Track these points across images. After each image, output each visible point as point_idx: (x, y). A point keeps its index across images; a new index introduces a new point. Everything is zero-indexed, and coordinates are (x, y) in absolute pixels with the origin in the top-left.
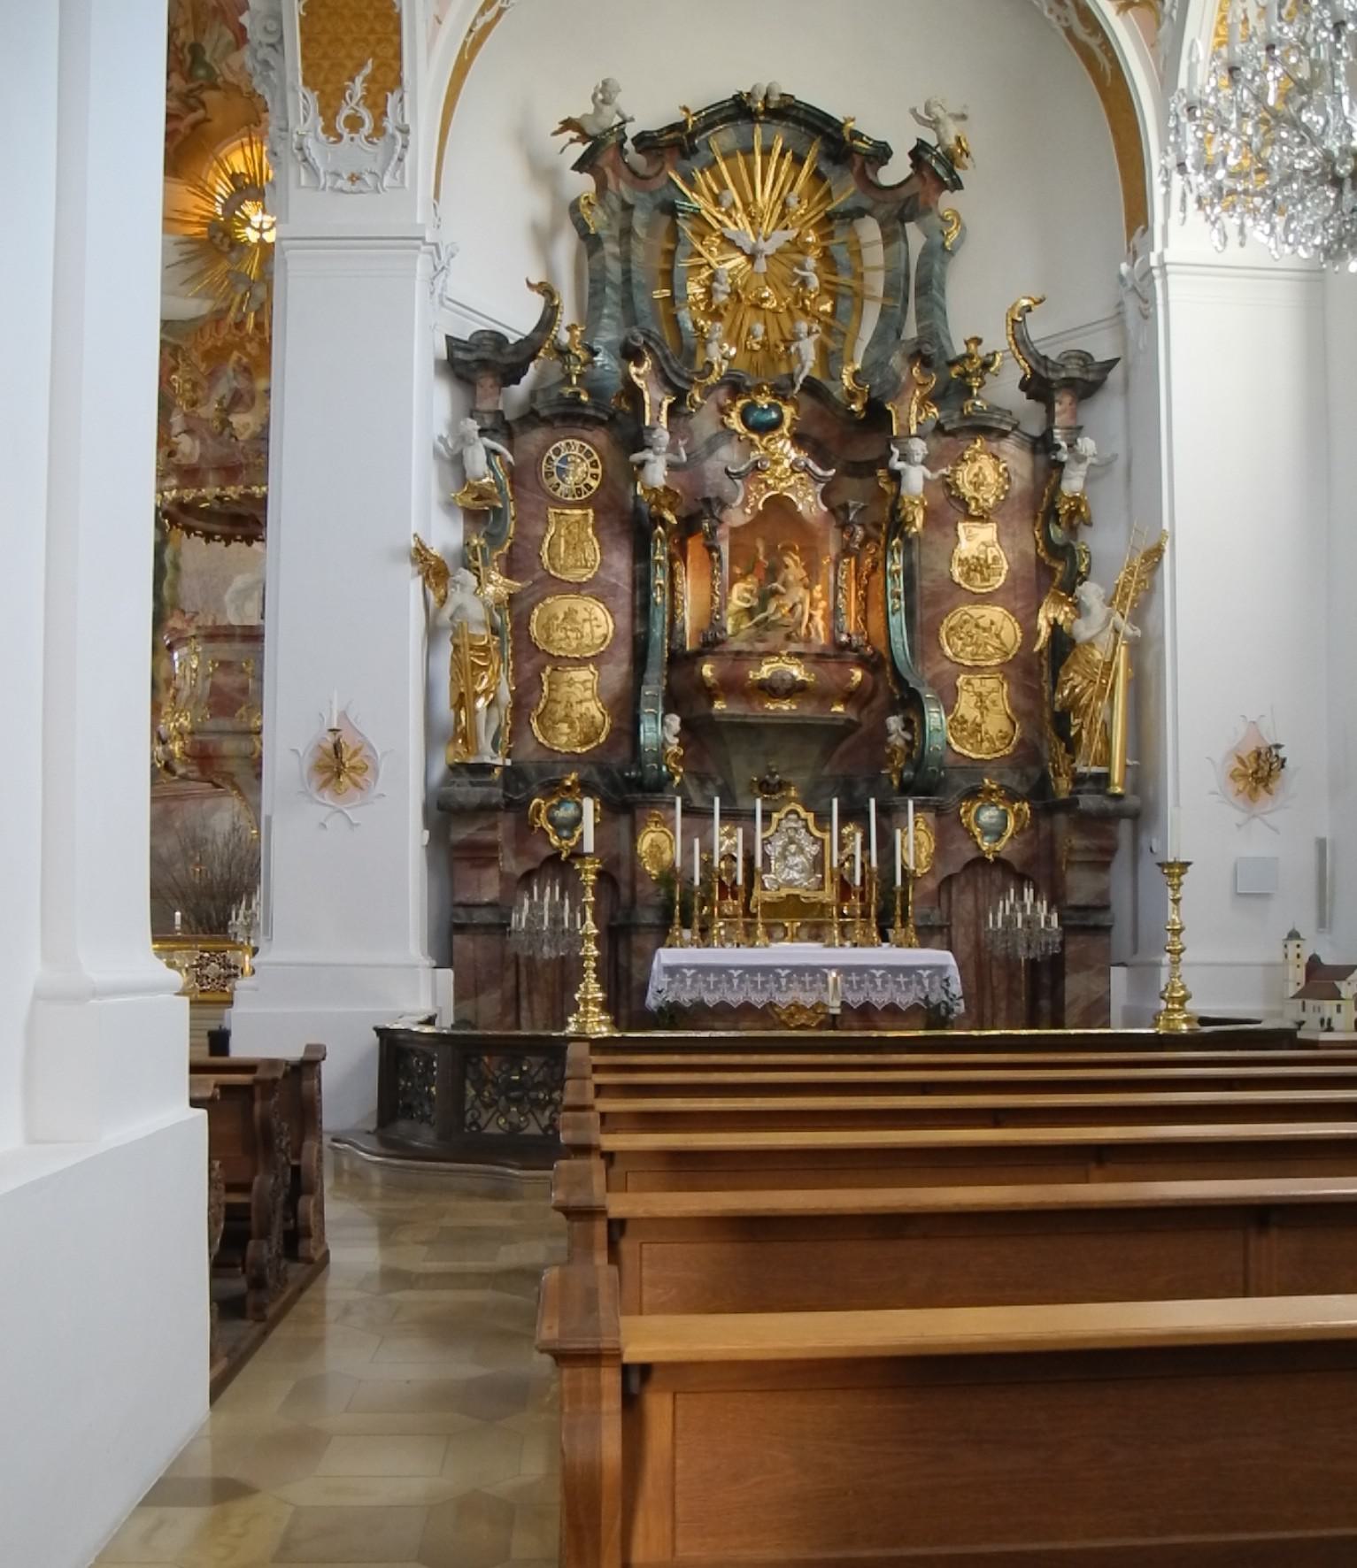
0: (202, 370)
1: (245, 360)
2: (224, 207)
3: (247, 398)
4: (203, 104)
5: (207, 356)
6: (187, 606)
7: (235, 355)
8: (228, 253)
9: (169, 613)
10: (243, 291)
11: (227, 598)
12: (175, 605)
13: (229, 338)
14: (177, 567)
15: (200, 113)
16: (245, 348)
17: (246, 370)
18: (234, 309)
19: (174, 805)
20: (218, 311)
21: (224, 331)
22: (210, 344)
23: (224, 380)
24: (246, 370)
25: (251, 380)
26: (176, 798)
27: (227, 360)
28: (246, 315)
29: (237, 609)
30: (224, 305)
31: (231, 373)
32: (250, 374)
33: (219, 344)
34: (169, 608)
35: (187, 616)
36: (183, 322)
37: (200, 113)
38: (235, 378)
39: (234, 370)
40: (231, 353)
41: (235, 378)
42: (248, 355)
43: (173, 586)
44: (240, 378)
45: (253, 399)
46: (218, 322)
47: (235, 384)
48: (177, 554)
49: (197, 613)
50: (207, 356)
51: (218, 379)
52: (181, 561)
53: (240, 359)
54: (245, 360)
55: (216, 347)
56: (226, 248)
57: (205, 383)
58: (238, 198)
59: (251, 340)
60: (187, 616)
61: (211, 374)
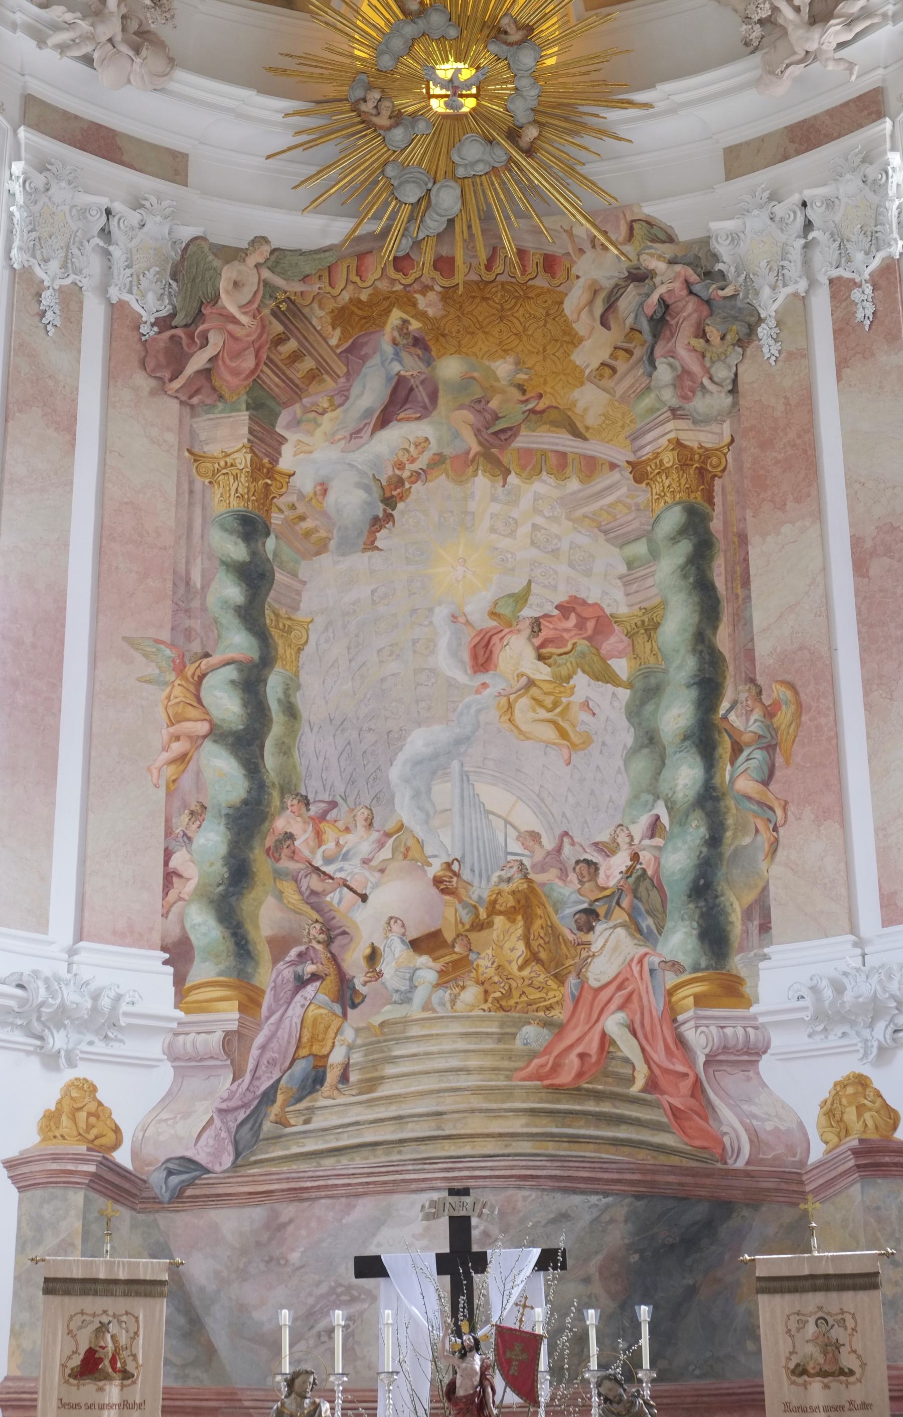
0: (333, 342)
1: (415, 325)
2: (379, 49)
3: (422, 394)
5: (341, 317)
6: (312, 788)
7: (396, 316)
8: (389, 129)
9: (276, 801)
10: (413, 200)
11: (395, 773)
12: (287, 789)
13: (383, 285)
14: (291, 712)
16: (414, 305)
17: (418, 342)
18: (394, 233)
19: (288, 1211)
20: (360, 239)
21: (373, 275)
22: (346, 296)
23: (375, 360)
24: (418, 342)
25: (429, 362)
26: (297, 1194)
27: (382, 326)
28: (417, 244)
29: (416, 795)
30: (377, 227)
31: (388, 349)
32: (426, 349)
33: (364, 297)
34: (275, 794)
35: (314, 810)
36: (302, 253)
38: (397, 357)
39: (395, 343)
40: (387, 312)
41: (397, 357)
42: (422, 316)
43: (285, 750)
44: (404, 355)
45: (434, 396)
46: (361, 257)
47: (396, 367)
48: (291, 686)
49: (333, 805)
50: (341, 317)
51: (365, 359)
52: (299, 700)
53: (405, 322)
54: (415, 325)
55: (358, 303)
56: (383, 120)
57: (340, 369)
58: (410, 30)
59: (426, 289)
60: (314, 810)
61: (348, 350)
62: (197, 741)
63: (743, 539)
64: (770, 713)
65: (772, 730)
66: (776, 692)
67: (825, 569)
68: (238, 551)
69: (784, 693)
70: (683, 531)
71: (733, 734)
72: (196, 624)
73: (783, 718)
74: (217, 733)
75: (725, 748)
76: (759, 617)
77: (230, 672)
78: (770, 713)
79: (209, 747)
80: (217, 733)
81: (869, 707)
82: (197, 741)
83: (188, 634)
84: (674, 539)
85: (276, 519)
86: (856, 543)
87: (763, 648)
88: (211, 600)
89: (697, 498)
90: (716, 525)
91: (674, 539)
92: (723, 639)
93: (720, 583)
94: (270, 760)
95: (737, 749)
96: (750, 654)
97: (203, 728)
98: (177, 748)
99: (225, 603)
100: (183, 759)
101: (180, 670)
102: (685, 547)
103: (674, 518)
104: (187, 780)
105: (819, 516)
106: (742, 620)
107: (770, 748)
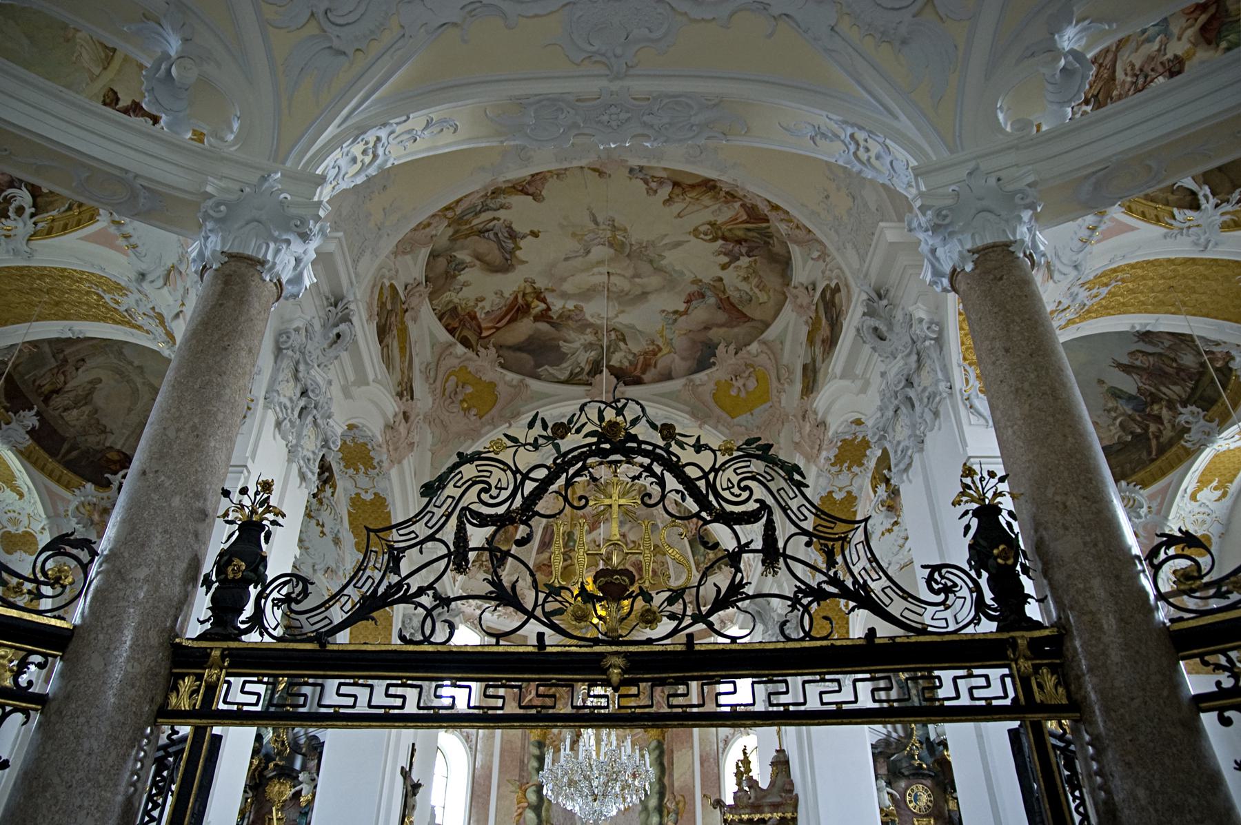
4: (571, 558)
15: (569, 562)
37: (569, 562)
43: (547, 810)
62: (524, 808)
63: (672, 751)
64: (677, 804)
65: (678, 809)
66: (679, 798)
67: (693, 763)
68: (536, 752)
69: (681, 798)
70: (657, 748)
71: (667, 808)
72: (525, 774)
73: (681, 805)
74: (530, 806)
75: (665, 813)
76: (675, 776)
77: (534, 788)
78: (677, 804)
79: (527, 810)
80: (530, 806)
81: (702, 805)
82: (524, 808)
83: (523, 777)
84: (654, 750)
85: (547, 742)
86: (701, 756)
87: (676, 784)
88: (530, 767)
89: (660, 738)
90: (665, 746)
91: (654, 750)
92: (666, 780)
93: (666, 764)
94: (543, 813)
95: (669, 813)
96: (673, 786)
97: (526, 804)
98: (519, 811)
99: (533, 767)
100: (520, 814)
101: (520, 788)
102: (657, 752)
103: (654, 744)
104: (522, 820)
105: (692, 747)
106: (671, 775)
107: (677, 814)
